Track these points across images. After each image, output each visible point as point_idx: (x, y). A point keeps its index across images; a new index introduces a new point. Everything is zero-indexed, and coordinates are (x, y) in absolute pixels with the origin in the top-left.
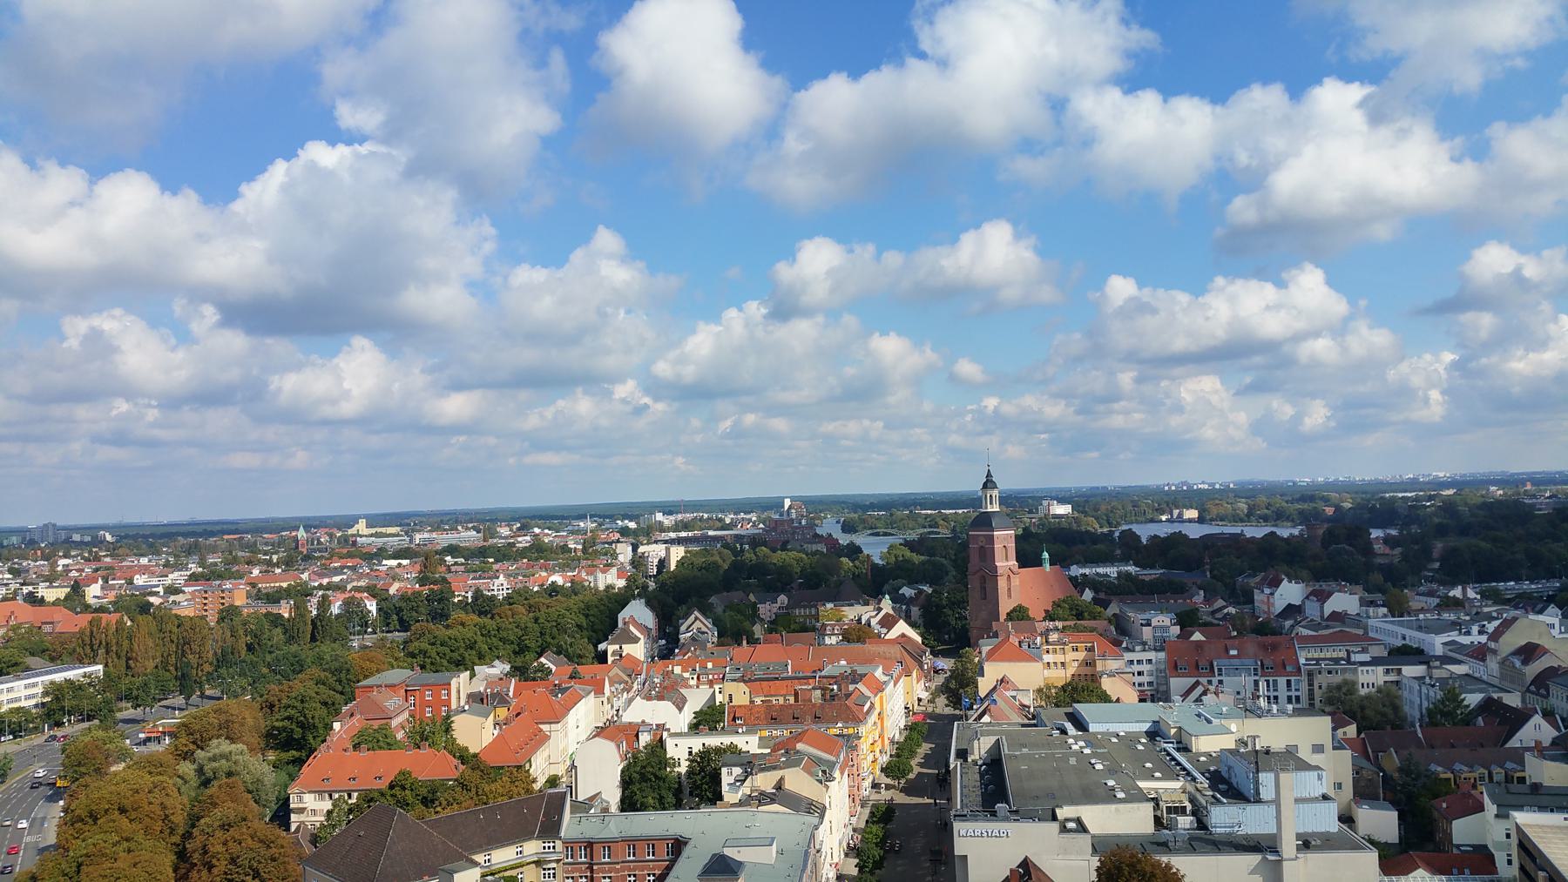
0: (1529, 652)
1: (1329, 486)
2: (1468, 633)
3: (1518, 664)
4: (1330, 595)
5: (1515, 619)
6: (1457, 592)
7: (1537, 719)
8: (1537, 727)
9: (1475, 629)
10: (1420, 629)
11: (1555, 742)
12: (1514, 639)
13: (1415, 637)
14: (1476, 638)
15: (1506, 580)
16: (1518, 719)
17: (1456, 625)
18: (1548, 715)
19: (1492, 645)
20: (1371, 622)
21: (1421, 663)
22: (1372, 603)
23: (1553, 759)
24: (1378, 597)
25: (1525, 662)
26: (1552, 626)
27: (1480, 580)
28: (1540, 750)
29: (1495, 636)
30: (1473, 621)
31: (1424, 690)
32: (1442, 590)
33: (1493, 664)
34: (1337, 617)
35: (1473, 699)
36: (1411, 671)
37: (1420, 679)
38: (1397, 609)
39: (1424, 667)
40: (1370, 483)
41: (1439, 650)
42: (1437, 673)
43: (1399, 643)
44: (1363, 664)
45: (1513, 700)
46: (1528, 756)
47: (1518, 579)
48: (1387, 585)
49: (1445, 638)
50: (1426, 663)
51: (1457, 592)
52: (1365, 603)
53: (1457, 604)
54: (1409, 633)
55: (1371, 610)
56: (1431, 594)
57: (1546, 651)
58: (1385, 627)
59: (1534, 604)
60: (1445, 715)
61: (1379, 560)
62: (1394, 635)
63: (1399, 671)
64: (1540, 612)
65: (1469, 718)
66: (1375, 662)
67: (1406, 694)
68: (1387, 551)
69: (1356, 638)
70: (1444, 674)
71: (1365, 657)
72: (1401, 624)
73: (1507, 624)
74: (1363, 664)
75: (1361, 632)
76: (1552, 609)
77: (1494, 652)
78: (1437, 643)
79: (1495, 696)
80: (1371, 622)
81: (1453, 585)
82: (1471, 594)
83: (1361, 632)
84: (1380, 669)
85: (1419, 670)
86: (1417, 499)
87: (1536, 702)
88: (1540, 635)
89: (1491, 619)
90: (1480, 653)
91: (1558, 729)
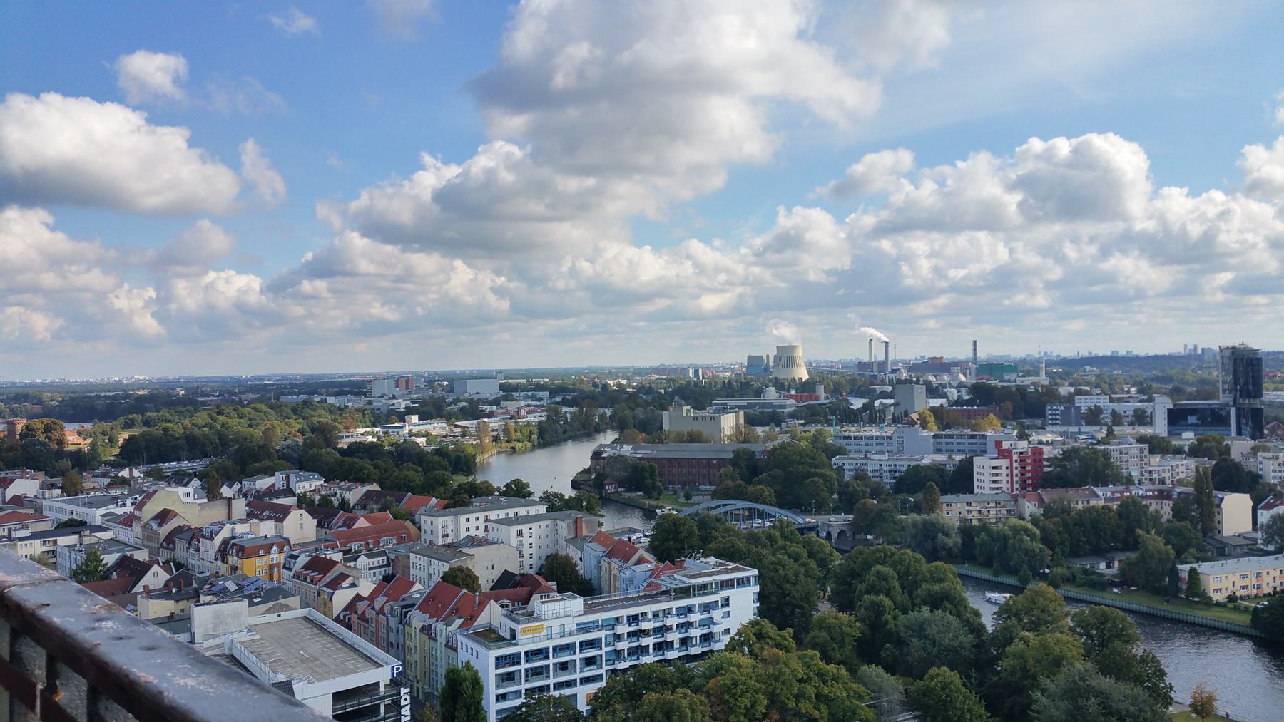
0: (164, 516)
1: (43, 386)
2: (124, 505)
3: (155, 526)
4: (12, 481)
5: (155, 491)
6: (125, 473)
7: (155, 568)
8: (156, 574)
9: (129, 501)
10: (84, 505)
11: (167, 584)
12: (152, 508)
13: (80, 512)
14: (129, 508)
15: (170, 461)
16: (143, 568)
17: (114, 500)
18: (166, 566)
19: (138, 513)
20: (45, 502)
21: (74, 533)
22: (53, 486)
23: (158, 597)
24: (59, 481)
25: (160, 525)
26: (187, 495)
27: (151, 461)
28: (148, 593)
29: (139, 506)
30: (129, 495)
31: (73, 556)
32: (113, 472)
33: (137, 528)
34: (18, 500)
35: (110, 559)
36: (64, 541)
37: (71, 547)
38: (70, 489)
39: (77, 536)
40: (82, 385)
41: (98, 521)
42: (86, 541)
43: (66, 518)
44: (21, 539)
45: (142, 556)
46: (139, 598)
47: (179, 460)
48: (66, 469)
49: (104, 511)
50: (79, 533)
51: (125, 473)
52: (43, 486)
53: (124, 481)
54: (75, 508)
55: (47, 492)
56: (104, 475)
57: (176, 515)
58: (58, 506)
59: (181, 478)
60: (84, 572)
61: (71, 448)
62: (63, 511)
63: (55, 542)
64: (186, 485)
65: (106, 576)
66: (34, 536)
67: (59, 560)
68: (81, 441)
69: (28, 517)
70: (94, 540)
71: (26, 533)
72: (70, 502)
73: (149, 496)
74: (21, 539)
75: (31, 511)
76: (196, 483)
77: (139, 519)
78: (96, 516)
79: (128, 554)
80: (45, 502)
81: (122, 466)
82: (136, 473)
83: (31, 511)
84: (38, 542)
85: (72, 539)
86: (116, 397)
87: (164, 555)
88: (174, 503)
89: (142, 492)
90: (128, 521)
91: (170, 572)
